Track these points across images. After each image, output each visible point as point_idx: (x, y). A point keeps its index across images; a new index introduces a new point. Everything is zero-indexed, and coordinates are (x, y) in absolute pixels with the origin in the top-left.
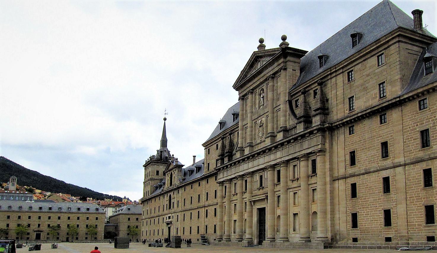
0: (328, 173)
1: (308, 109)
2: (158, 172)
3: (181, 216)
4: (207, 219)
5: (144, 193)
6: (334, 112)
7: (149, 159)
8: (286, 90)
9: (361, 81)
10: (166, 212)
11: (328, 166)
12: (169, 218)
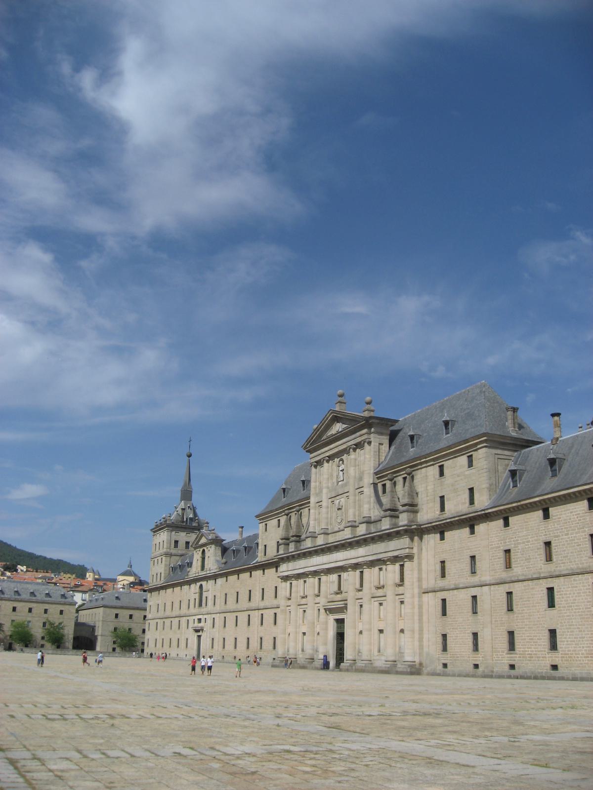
0: (416, 584)
2: (176, 542)
3: (219, 619)
4: (263, 628)
7: (163, 520)
8: (370, 470)
10: (192, 610)
12: (200, 620)
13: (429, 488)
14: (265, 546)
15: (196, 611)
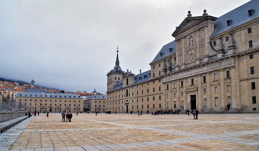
1: (223, 46)
2: (116, 78)
4: (154, 101)
5: (108, 89)
6: (240, 48)
7: (110, 72)
9: (256, 34)
11: (237, 74)
12: (127, 101)
13: (241, 39)
14: (154, 74)
15: (126, 97)
